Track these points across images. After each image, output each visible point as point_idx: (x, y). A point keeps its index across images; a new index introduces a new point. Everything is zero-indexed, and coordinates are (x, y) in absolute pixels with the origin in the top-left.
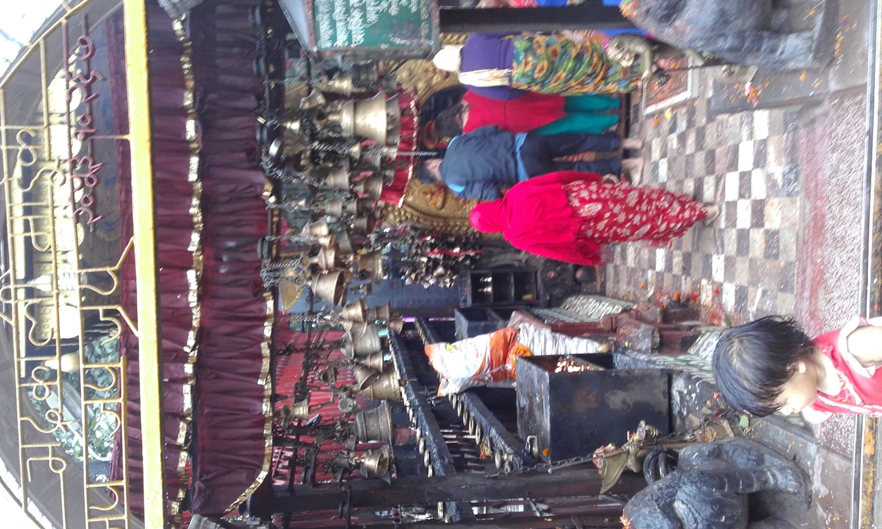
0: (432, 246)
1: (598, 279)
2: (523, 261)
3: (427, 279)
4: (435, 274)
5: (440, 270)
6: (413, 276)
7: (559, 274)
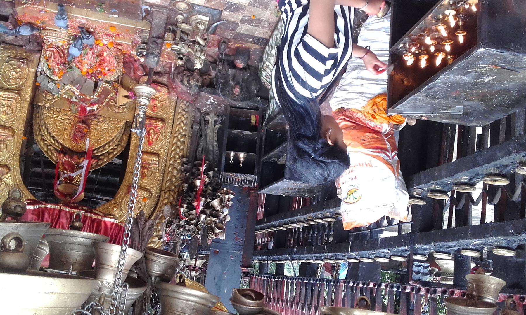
0: (191, 207)
1: (248, 45)
2: (216, 118)
3: (222, 217)
4: (218, 208)
5: (216, 203)
6: (218, 231)
7: (238, 83)
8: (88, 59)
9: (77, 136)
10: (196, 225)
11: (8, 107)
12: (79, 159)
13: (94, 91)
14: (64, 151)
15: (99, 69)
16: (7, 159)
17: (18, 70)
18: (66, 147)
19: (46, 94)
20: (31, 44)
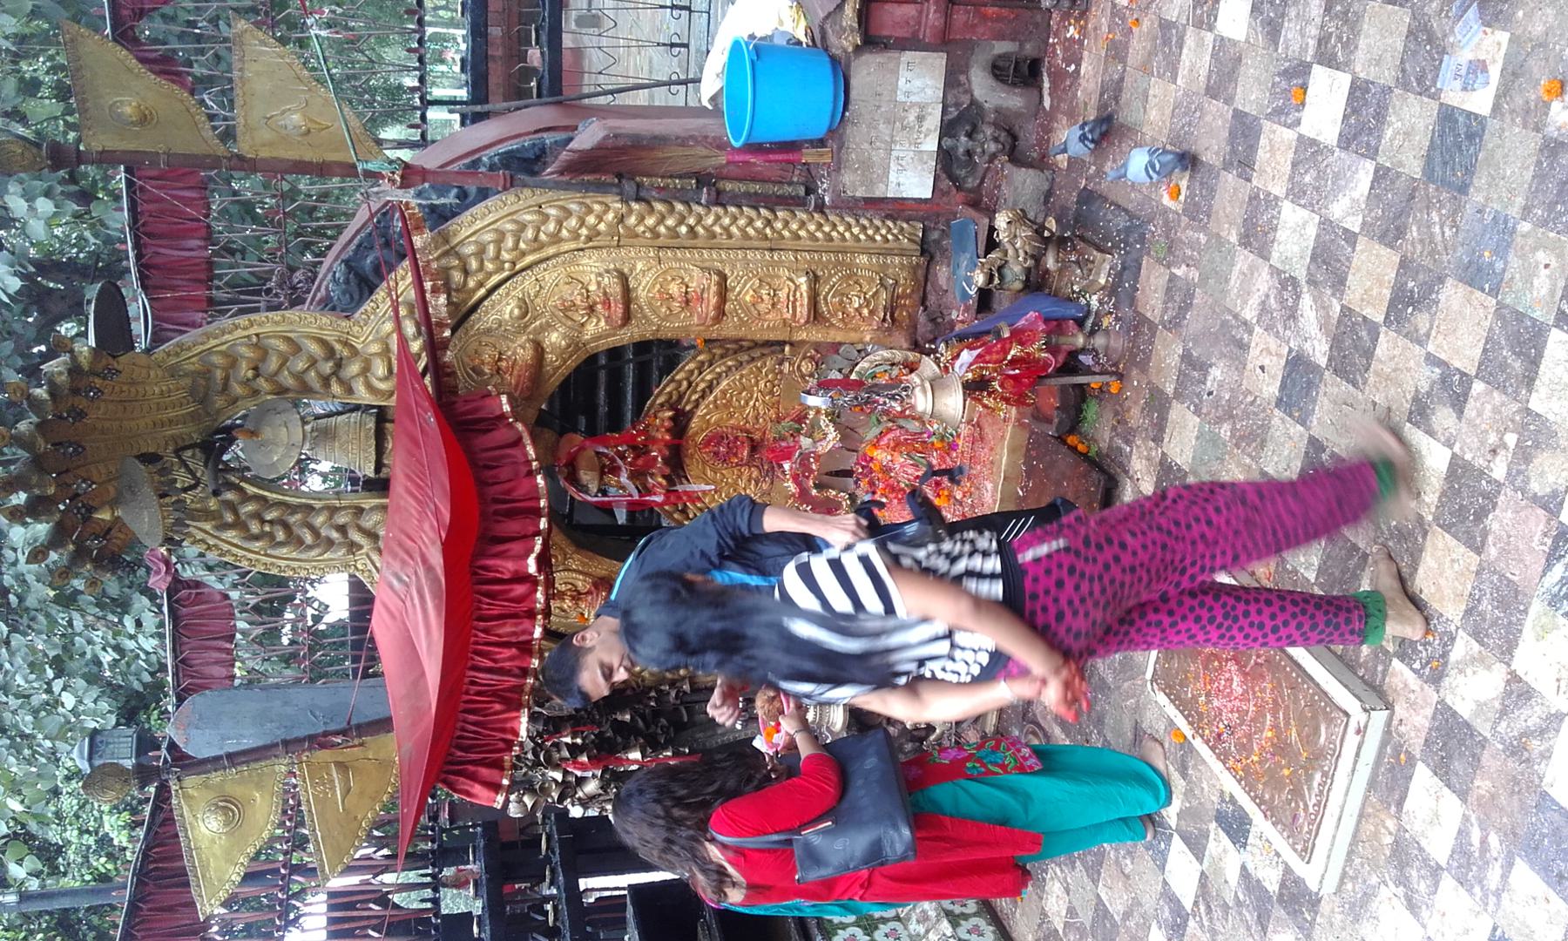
4: (580, 794)
8: (902, 466)
9: (718, 444)
10: (537, 764)
11: (773, 305)
12: (664, 477)
13: (830, 474)
14: (681, 421)
15: (881, 485)
16: (645, 317)
17: (865, 312)
18: (690, 420)
19: (812, 358)
20: (930, 326)
